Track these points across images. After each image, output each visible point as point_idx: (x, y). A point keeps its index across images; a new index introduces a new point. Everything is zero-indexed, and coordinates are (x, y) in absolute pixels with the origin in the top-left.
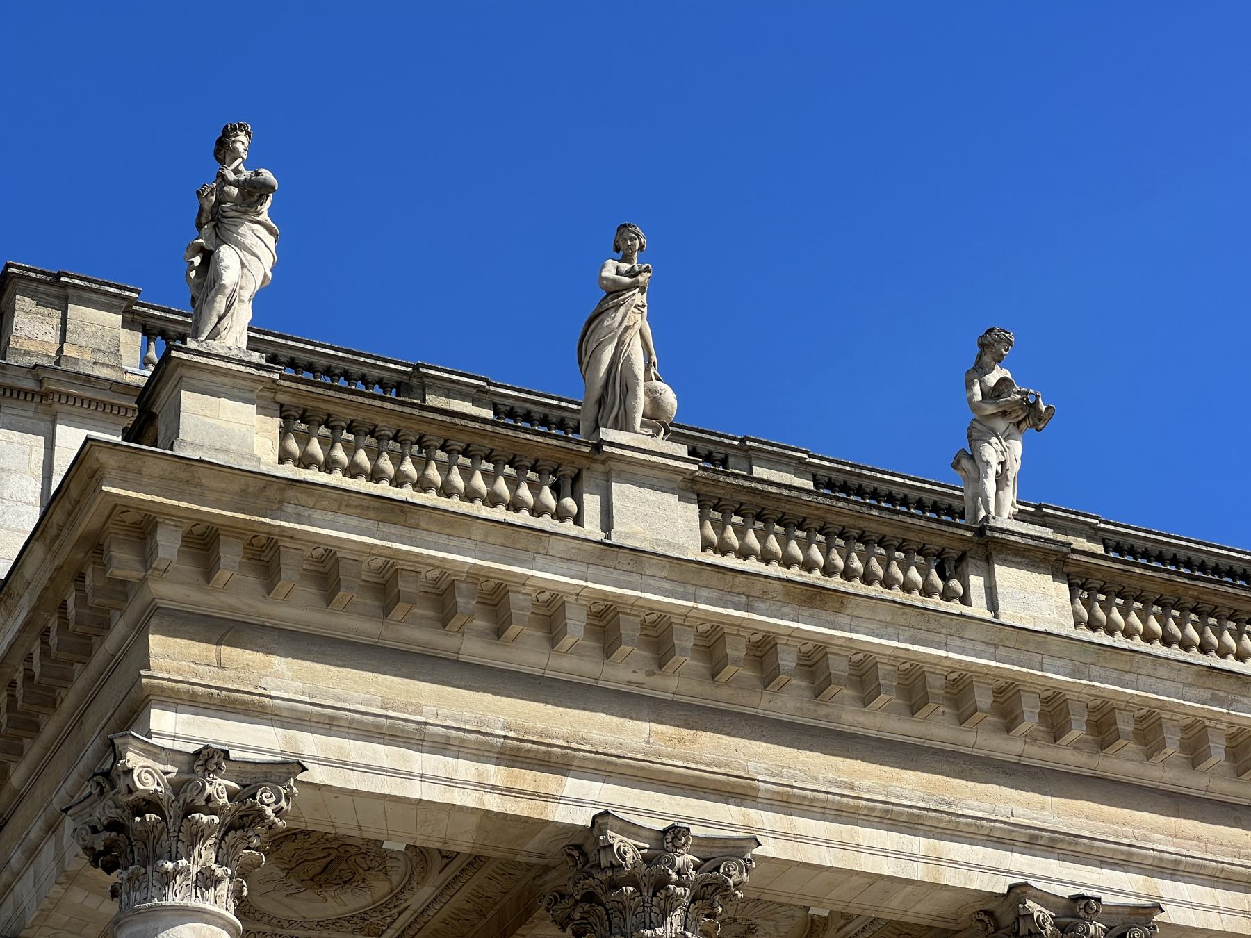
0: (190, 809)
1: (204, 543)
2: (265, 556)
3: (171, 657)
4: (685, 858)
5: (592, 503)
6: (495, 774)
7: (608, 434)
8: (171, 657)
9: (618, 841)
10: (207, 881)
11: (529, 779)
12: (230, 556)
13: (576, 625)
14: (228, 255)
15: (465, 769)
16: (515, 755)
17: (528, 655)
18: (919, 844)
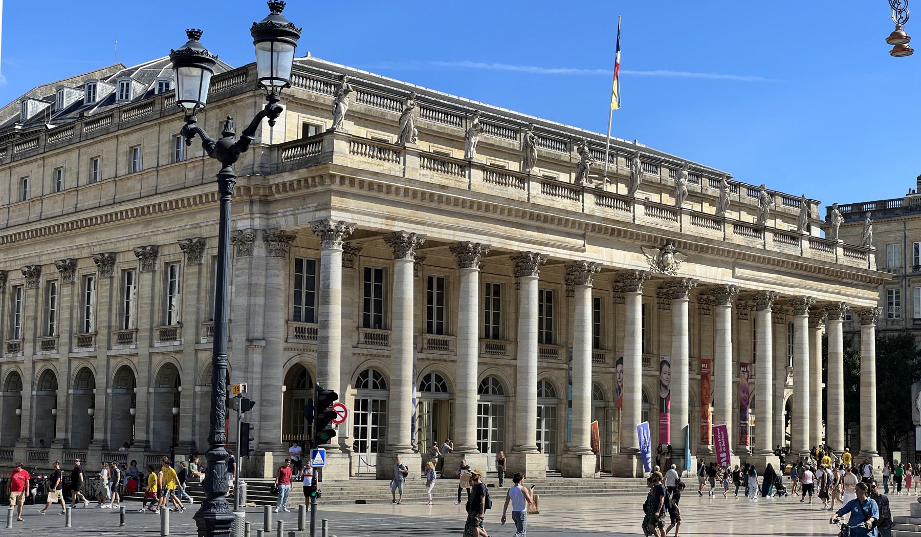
0: (338, 232)
1: (342, 179)
2: (352, 181)
3: (335, 200)
4: (415, 238)
5: (402, 158)
6: (384, 221)
7: (407, 145)
8: (335, 200)
9: (404, 235)
10: (340, 244)
11: (390, 222)
12: (347, 182)
13: (402, 192)
14: (341, 104)
15: (379, 220)
16: (388, 218)
17: (392, 197)
18: (452, 232)
